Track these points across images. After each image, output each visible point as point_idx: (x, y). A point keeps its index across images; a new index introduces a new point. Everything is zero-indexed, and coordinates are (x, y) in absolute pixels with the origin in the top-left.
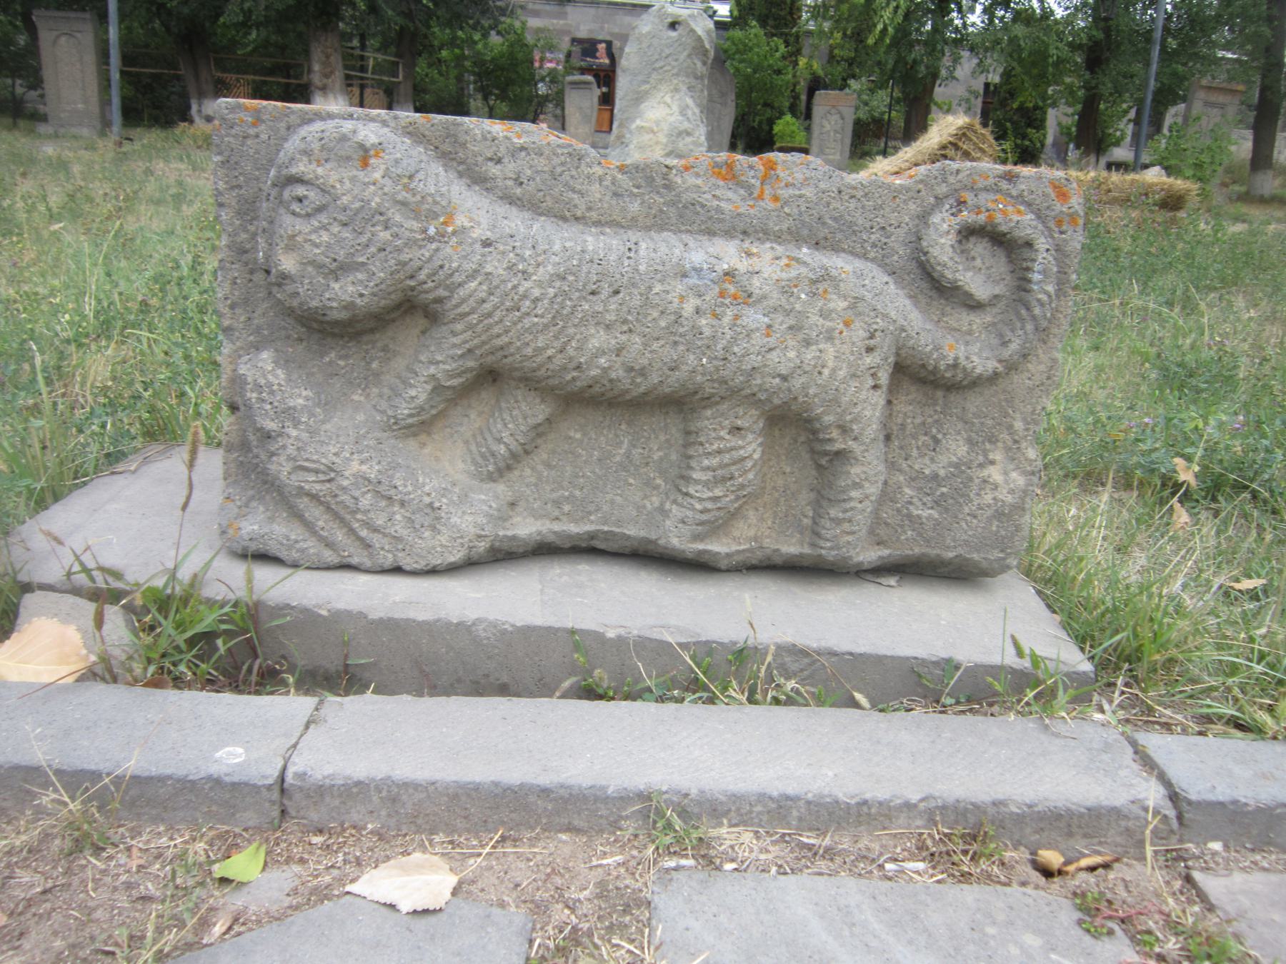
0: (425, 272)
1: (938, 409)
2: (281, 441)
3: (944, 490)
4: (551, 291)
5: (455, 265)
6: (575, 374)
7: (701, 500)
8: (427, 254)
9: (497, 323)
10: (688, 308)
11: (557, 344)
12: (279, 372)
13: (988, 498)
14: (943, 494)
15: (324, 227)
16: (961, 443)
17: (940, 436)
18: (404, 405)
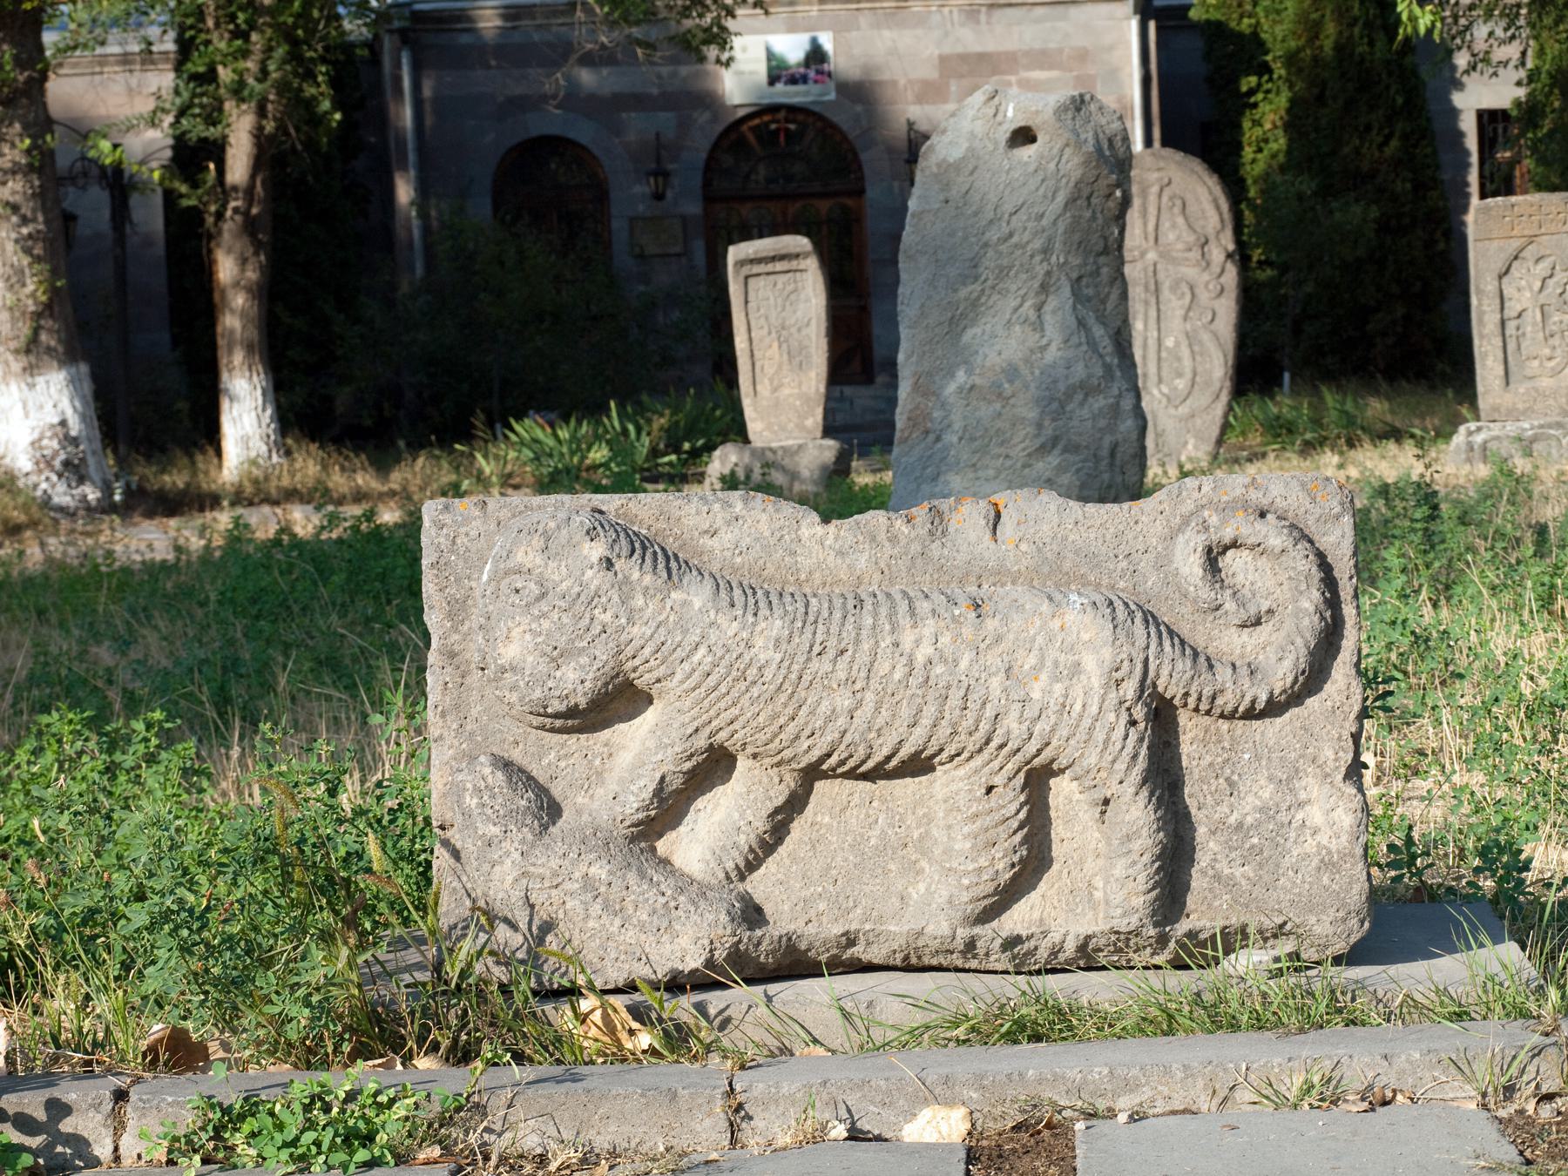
0: (647, 651)
1: (1226, 745)
2: (506, 845)
3: (1255, 840)
4: (778, 657)
5: (679, 638)
6: (810, 742)
7: (966, 873)
8: (649, 632)
9: (724, 696)
10: (920, 659)
11: (790, 711)
12: (499, 774)
13: (1310, 845)
14: (1253, 847)
15: (544, 615)
16: (1263, 782)
17: (1235, 777)
18: (632, 798)
